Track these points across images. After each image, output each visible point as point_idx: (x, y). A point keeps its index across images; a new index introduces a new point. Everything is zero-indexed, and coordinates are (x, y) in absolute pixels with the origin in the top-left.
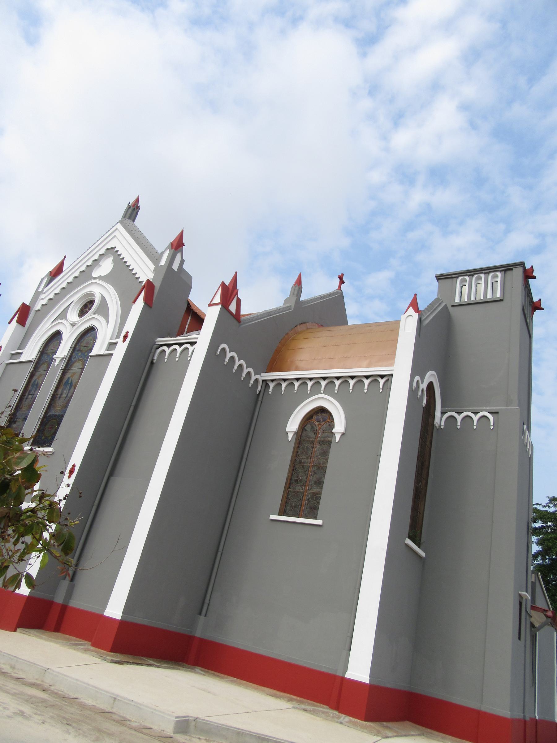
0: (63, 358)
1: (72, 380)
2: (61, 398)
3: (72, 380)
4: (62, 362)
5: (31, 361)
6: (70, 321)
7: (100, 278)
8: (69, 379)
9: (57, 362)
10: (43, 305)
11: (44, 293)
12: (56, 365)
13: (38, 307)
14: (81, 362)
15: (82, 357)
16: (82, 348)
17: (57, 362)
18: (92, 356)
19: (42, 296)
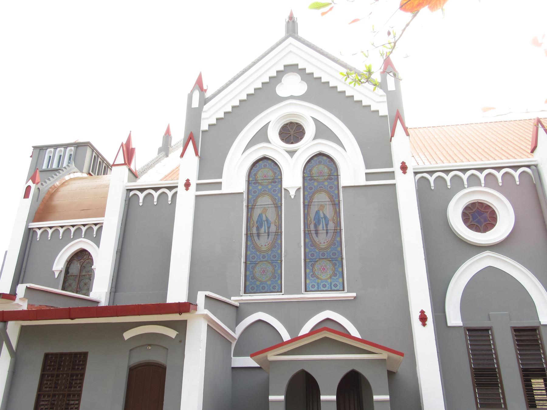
0: (299, 189)
1: (324, 214)
2: (320, 235)
3: (324, 214)
4: (300, 192)
5: (242, 193)
6: (282, 147)
7: (292, 97)
8: (317, 213)
9: (292, 193)
10: (210, 126)
11: (205, 112)
12: (293, 197)
13: (204, 126)
14: (323, 193)
15: (322, 187)
16: (315, 178)
17: (292, 193)
18: (343, 187)
19: (203, 115)
